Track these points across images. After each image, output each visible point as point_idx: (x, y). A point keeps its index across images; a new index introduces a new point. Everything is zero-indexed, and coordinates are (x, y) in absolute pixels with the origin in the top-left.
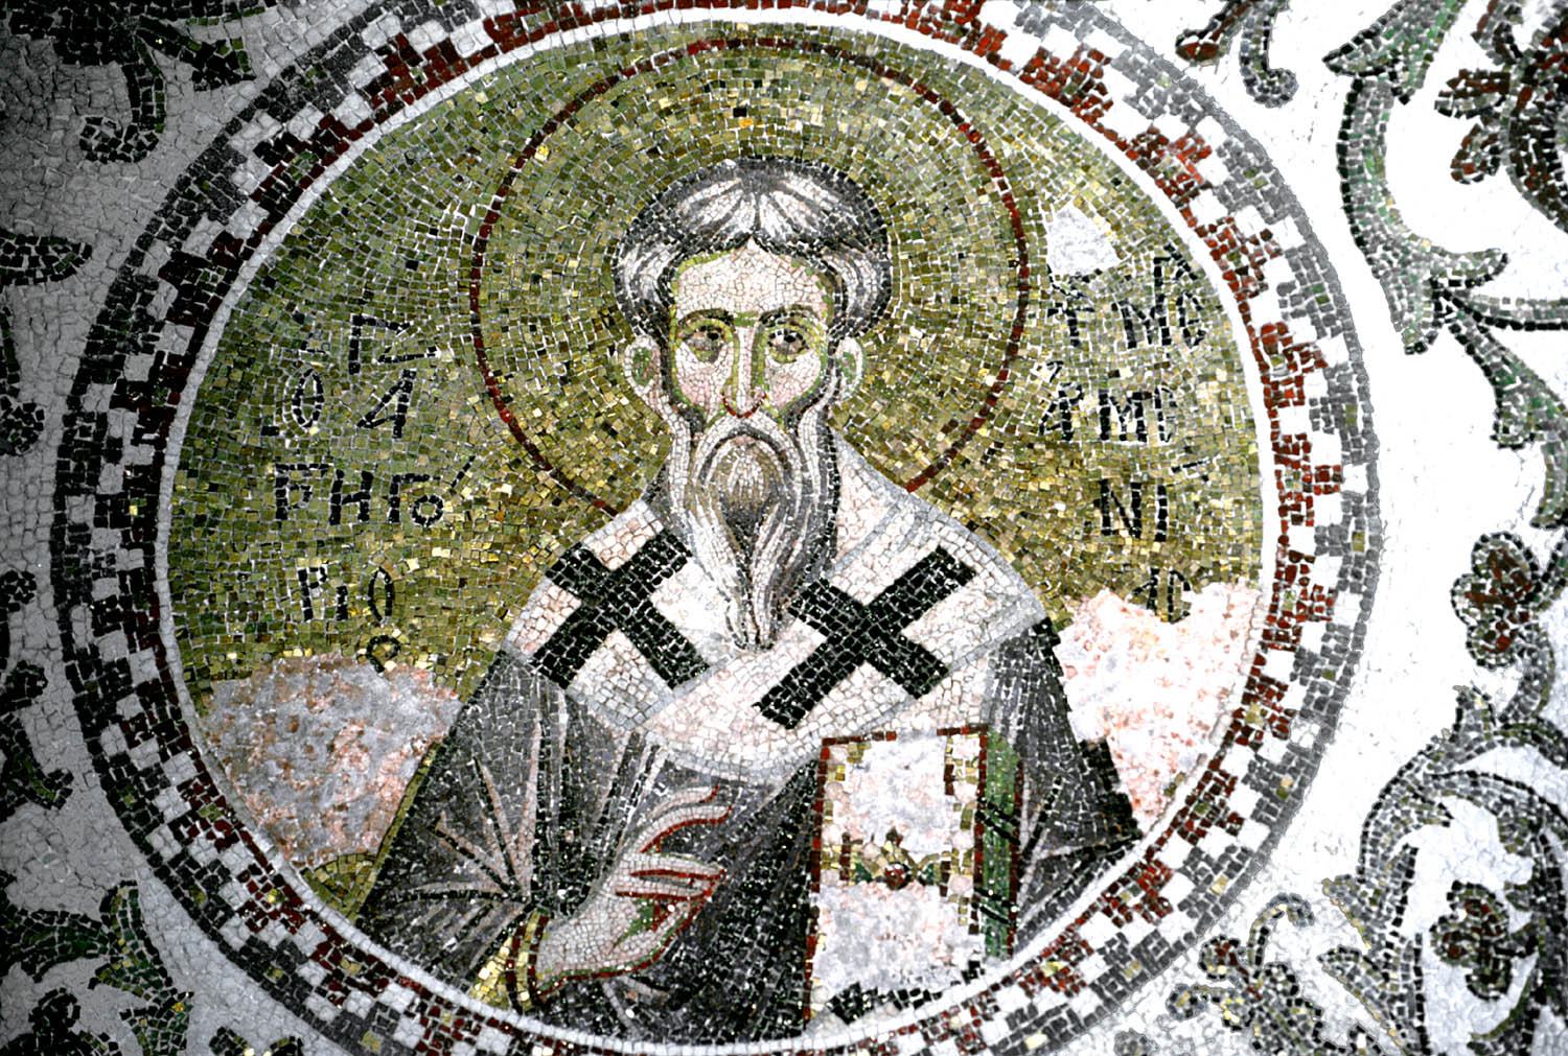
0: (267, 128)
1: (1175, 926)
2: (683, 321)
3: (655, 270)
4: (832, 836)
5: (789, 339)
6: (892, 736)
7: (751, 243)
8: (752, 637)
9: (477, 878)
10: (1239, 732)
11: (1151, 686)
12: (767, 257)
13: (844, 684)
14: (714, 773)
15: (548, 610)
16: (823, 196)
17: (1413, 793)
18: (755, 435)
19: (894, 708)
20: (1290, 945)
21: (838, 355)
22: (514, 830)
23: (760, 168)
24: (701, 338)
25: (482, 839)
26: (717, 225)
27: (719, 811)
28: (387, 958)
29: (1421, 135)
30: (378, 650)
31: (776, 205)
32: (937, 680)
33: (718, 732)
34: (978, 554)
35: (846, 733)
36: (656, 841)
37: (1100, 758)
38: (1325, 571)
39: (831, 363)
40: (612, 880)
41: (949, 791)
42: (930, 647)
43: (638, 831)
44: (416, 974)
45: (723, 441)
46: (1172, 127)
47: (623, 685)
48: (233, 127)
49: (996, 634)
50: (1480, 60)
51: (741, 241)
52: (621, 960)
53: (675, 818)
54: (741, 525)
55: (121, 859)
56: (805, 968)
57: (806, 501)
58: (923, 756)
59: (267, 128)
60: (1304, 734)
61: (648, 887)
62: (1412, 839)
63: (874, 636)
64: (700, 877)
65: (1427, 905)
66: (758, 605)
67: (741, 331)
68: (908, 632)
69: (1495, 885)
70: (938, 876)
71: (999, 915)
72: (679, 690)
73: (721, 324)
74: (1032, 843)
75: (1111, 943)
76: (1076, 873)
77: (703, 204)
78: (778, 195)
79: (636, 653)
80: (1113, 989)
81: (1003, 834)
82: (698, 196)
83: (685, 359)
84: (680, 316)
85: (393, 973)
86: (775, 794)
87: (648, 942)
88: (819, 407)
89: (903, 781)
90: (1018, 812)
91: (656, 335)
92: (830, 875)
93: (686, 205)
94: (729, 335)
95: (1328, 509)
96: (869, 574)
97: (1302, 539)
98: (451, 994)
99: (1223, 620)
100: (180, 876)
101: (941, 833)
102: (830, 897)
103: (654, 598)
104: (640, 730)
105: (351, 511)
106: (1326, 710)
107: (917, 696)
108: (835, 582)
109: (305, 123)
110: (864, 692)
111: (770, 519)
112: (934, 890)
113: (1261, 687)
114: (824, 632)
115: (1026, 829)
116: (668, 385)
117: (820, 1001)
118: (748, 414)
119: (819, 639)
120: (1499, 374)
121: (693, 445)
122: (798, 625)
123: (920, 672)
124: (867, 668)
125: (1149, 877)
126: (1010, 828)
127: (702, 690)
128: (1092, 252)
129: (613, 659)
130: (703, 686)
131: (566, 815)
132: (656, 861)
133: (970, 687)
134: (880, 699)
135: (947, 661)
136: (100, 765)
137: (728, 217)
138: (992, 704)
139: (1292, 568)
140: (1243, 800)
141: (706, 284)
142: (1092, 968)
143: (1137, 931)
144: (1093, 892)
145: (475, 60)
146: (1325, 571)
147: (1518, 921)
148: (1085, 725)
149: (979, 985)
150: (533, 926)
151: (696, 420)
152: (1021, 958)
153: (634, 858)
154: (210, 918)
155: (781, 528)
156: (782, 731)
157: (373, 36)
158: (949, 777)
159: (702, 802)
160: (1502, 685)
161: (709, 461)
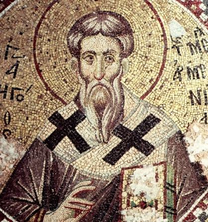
2: (84, 53)
3: (76, 40)
4: (124, 194)
5: (110, 59)
6: (142, 167)
7: (100, 34)
8: (102, 140)
9: (28, 198)
12: (104, 37)
13: (127, 153)
14: (92, 177)
15: (50, 129)
16: (116, 21)
18: (102, 85)
19: (141, 159)
21: (122, 63)
22: (38, 186)
23: (101, 15)
24: (88, 59)
26: (92, 29)
27: (92, 188)
28: (3, 212)
30: (6, 133)
31: (106, 24)
32: (152, 151)
33: (91, 166)
34: (160, 115)
35: (127, 166)
36: (76, 194)
39: (121, 65)
40: (64, 203)
41: (157, 180)
42: (150, 142)
43: (71, 191)
45: (94, 86)
47: (67, 151)
51: (98, 33)
53: (81, 189)
57: (115, 104)
58: (149, 173)
61: (74, 206)
63: (134, 139)
64: (87, 205)
67: (98, 57)
68: (144, 138)
70: (154, 204)
72: (83, 154)
73: (93, 55)
74: (180, 192)
75: (202, 215)
76: (192, 199)
77: (88, 23)
78: (106, 21)
79: (71, 143)
81: (172, 191)
82: (87, 21)
83: (84, 63)
84: (83, 52)
85: (5, 217)
86: (109, 183)
88: (118, 77)
90: (175, 185)
91: (77, 57)
94: (95, 58)
96: (133, 122)
101: (155, 192)
103: (76, 128)
104: (71, 164)
107: (147, 156)
108: (124, 125)
110: (132, 155)
111: (107, 107)
112: (154, 209)
114: (121, 138)
115: (178, 188)
116: (80, 71)
118: (99, 79)
119: (120, 140)
121: (86, 87)
122: (114, 137)
123: (147, 149)
124: (133, 148)
126: (173, 189)
127: (89, 154)
128: (180, 31)
129: (65, 147)
130: (88, 154)
132: (76, 200)
133: (160, 153)
134: (137, 156)
135: (154, 145)
137: (94, 27)
141: (88, 44)
148: (193, 159)
150: (42, 212)
151: (87, 81)
153: (70, 198)
155: (109, 110)
156: (111, 166)
158: (157, 176)
159: (88, 185)
161: (90, 92)
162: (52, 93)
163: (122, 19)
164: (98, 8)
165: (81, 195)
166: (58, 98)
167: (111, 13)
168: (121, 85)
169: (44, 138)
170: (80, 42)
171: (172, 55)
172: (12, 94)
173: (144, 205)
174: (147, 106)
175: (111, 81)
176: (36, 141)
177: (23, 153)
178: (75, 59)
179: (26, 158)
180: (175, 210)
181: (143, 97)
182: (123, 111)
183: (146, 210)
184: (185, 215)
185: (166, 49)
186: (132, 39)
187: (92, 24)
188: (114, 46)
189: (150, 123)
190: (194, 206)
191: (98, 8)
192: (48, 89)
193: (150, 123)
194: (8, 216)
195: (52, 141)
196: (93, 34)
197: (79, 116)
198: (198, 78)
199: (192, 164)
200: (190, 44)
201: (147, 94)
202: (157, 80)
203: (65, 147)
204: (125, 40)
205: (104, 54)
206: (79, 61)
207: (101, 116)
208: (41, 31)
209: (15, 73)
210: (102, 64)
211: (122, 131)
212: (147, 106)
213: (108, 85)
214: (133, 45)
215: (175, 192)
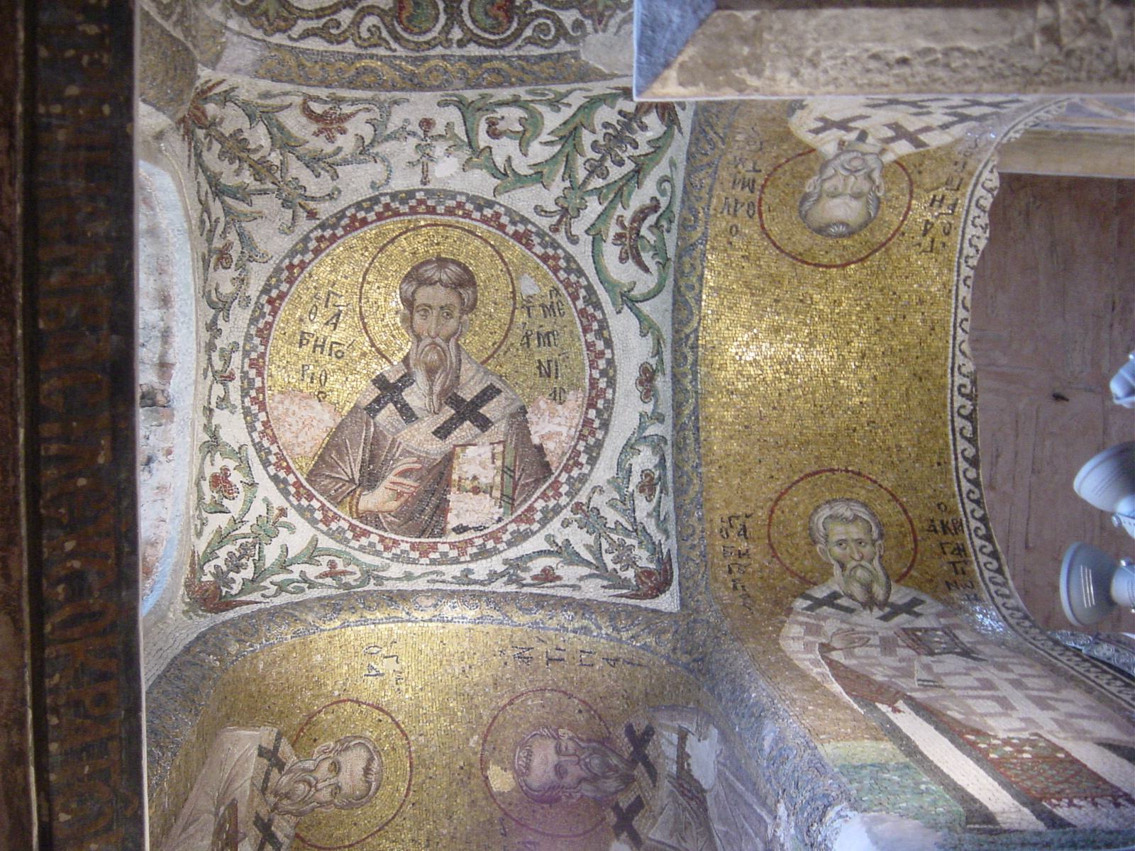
0: (319, 232)
1: (564, 500)
3: (411, 289)
4: (455, 477)
10: (581, 437)
11: (554, 427)
17: (630, 447)
19: (476, 436)
20: (599, 501)
25: (344, 462)
27: (418, 466)
29: (611, 252)
37: (540, 449)
38: (602, 384)
44: (322, 498)
46: (551, 252)
48: (311, 231)
49: (508, 411)
50: (619, 230)
52: (386, 508)
53: (405, 467)
54: (431, 372)
55: (244, 438)
56: (445, 517)
59: (319, 232)
60: (599, 435)
62: (632, 461)
63: (470, 412)
65: (636, 479)
66: (435, 398)
68: (481, 411)
69: (651, 467)
70: (489, 490)
71: (509, 501)
80: (544, 522)
83: (417, 317)
87: (394, 505)
89: (478, 459)
92: (454, 489)
93: (421, 271)
95: (602, 364)
97: (596, 374)
98: (332, 507)
99: (575, 400)
100: (259, 448)
101: (489, 476)
102: (453, 496)
105: (319, 349)
106: (605, 425)
109: (328, 233)
110: (467, 429)
113: (587, 422)
116: (412, 327)
117: (450, 527)
120: (638, 315)
123: (484, 424)
125: (556, 485)
129: (388, 414)
131: (371, 462)
133: (500, 429)
136: (243, 408)
138: (506, 435)
139: (593, 382)
140: (583, 459)
141: (424, 295)
142: (538, 516)
143: (552, 503)
144: (538, 493)
145: (372, 222)
146: (602, 384)
147: (657, 473)
148: (536, 440)
149: (502, 524)
151: (418, 338)
152: (516, 515)
154: (266, 463)
157: (348, 213)
160: (649, 408)
162: (378, 350)
163: (466, 269)
164: (439, 254)
165: (403, 474)
166: (384, 356)
167: (453, 262)
168: (458, 347)
169: (365, 403)
170: (413, 293)
171: (521, 317)
172: (331, 348)
173: (476, 490)
174: (486, 372)
175: (447, 340)
176: (356, 406)
177: (339, 420)
178: (407, 312)
179: (340, 427)
180: (513, 500)
181: (483, 363)
182: (458, 377)
183: (477, 497)
184: (525, 506)
185: (515, 308)
186: (475, 293)
187: (430, 272)
188: (453, 299)
189: (489, 394)
190: (535, 496)
191: (439, 254)
192: (373, 345)
193: (489, 394)
194: (318, 496)
195: (373, 409)
196: (431, 284)
197: (407, 380)
198: (549, 344)
199: (535, 446)
200: (543, 306)
201: (488, 358)
202: (502, 343)
203: (388, 414)
204: (467, 294)
205: (442, 308)
206: (411, 313)
207: (433, 381)
208: (370, 278)
209: (335, 325)
210: (438, 316)
211: (456, 401)
212: (486, 372)
213: (443, 345)
214: (476, 300)
215: (513, 477)
